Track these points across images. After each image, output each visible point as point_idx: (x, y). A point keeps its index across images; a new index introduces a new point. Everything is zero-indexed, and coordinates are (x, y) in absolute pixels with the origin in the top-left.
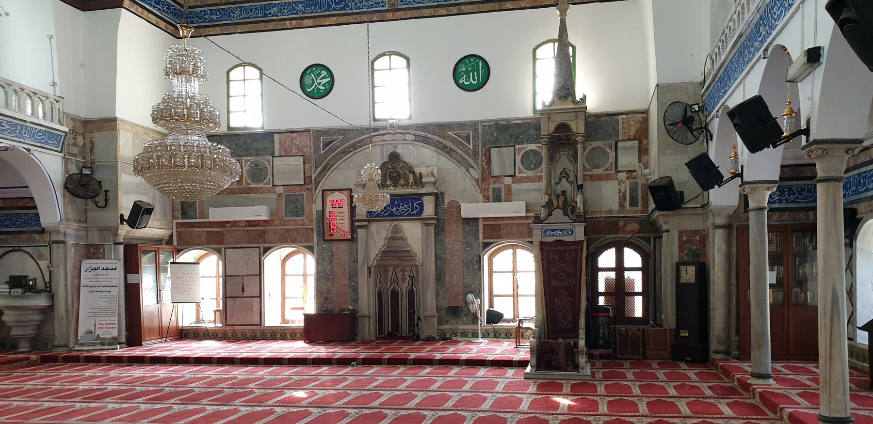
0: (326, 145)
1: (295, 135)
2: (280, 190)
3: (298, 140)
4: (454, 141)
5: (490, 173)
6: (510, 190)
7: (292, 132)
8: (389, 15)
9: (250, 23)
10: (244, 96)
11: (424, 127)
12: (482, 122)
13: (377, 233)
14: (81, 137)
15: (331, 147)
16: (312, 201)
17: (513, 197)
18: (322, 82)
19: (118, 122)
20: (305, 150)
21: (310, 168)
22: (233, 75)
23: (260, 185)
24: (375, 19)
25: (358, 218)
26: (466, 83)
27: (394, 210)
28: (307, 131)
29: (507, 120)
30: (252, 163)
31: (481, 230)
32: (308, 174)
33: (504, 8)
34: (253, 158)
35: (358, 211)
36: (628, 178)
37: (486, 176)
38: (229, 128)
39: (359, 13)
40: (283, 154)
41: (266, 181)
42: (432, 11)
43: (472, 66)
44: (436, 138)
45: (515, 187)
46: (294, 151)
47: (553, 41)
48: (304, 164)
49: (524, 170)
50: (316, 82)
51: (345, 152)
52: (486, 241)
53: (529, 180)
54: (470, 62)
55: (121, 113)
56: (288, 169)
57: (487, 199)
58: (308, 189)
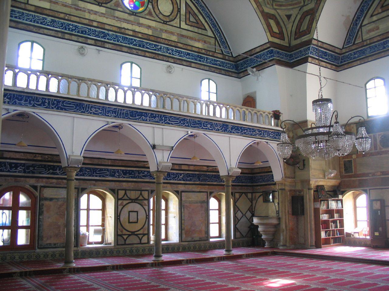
10: (376, 96)
14: (291, 132)
22: (368, 86)
30: (382, 136)
38: (368, 117)
55: (308, 118)
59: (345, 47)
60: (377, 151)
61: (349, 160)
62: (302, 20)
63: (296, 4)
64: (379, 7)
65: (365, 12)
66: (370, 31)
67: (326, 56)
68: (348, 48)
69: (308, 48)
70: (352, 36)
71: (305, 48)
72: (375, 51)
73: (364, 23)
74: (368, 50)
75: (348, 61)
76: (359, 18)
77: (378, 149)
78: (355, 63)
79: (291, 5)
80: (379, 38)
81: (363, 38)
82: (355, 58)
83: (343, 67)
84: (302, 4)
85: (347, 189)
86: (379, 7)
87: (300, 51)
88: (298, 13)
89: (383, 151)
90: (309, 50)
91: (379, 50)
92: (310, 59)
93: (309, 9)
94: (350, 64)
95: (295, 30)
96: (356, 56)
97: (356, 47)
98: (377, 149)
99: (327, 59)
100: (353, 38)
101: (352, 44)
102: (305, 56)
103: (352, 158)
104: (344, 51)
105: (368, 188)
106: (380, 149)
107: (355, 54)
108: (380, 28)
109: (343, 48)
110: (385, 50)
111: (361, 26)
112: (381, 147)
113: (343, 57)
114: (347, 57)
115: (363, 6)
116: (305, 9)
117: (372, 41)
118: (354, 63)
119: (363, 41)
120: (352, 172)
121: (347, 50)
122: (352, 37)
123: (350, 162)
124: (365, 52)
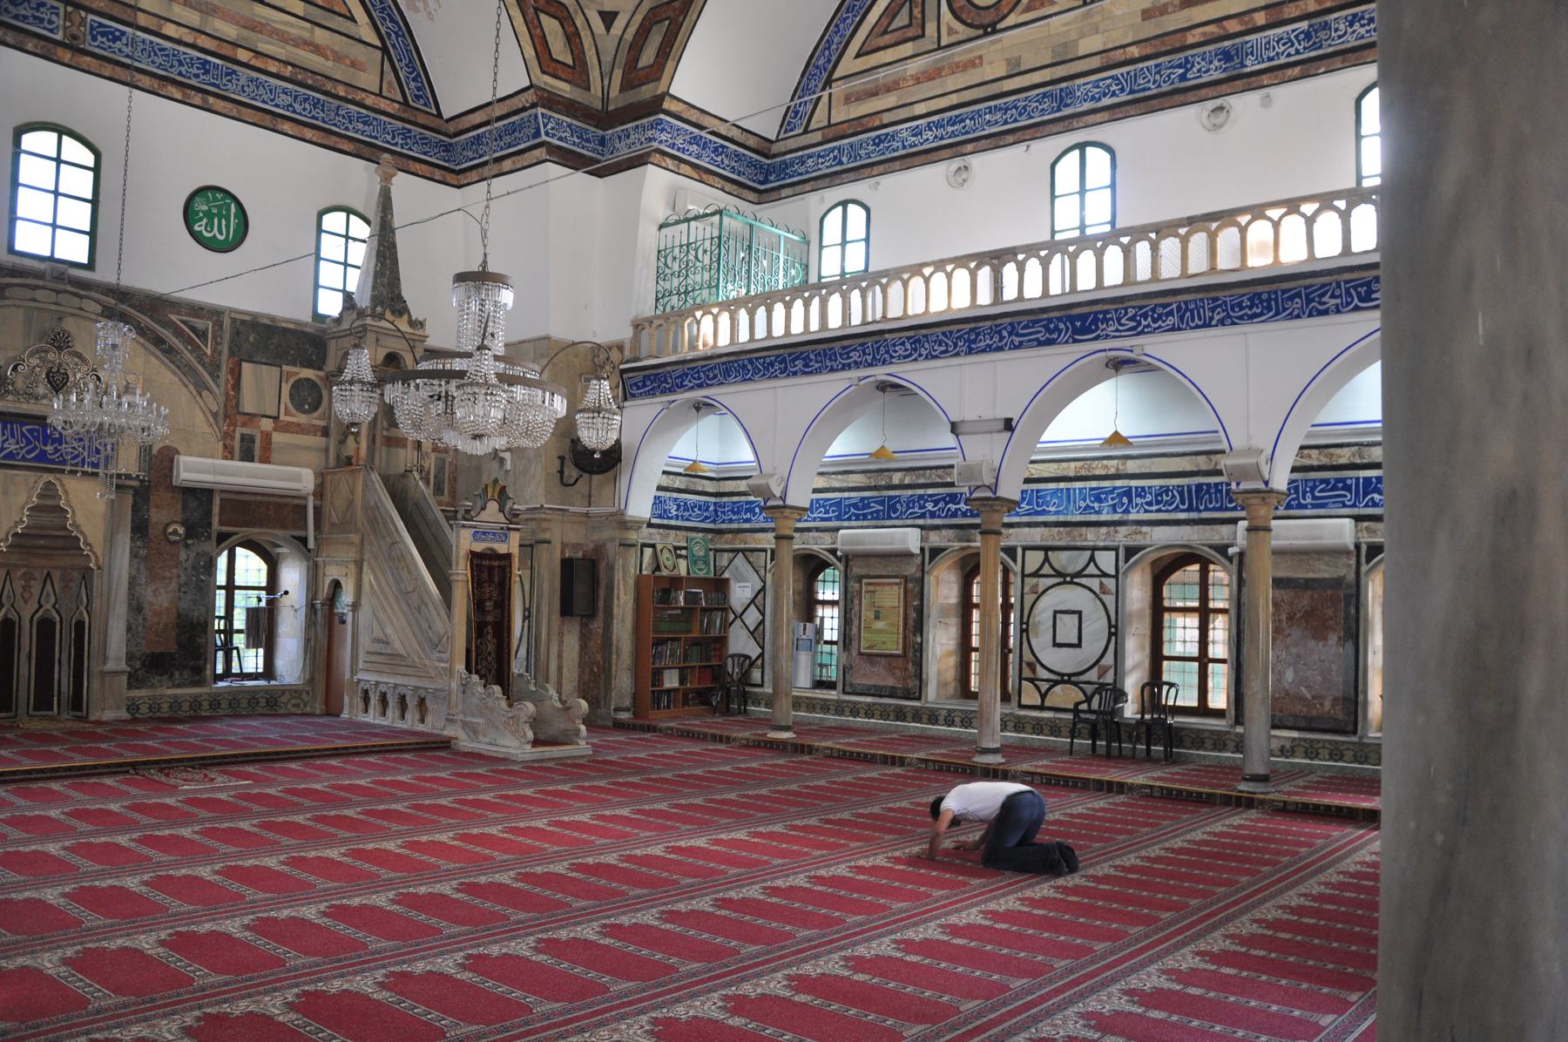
4: (178, 332)
5: (237, 404)
6: (270, 443)
11: (122, 294)
12: (232, 310)
17: (274, 456)
27: (49, 448)
29: (273, 319)
31: (216, 510)
33: (279, 127)
37: (231, 412)
44: (145, 320)
45: (278, 438)
47: (349, 211)
49: (293, 410)
54: (215, 199)
57: (229, 453)
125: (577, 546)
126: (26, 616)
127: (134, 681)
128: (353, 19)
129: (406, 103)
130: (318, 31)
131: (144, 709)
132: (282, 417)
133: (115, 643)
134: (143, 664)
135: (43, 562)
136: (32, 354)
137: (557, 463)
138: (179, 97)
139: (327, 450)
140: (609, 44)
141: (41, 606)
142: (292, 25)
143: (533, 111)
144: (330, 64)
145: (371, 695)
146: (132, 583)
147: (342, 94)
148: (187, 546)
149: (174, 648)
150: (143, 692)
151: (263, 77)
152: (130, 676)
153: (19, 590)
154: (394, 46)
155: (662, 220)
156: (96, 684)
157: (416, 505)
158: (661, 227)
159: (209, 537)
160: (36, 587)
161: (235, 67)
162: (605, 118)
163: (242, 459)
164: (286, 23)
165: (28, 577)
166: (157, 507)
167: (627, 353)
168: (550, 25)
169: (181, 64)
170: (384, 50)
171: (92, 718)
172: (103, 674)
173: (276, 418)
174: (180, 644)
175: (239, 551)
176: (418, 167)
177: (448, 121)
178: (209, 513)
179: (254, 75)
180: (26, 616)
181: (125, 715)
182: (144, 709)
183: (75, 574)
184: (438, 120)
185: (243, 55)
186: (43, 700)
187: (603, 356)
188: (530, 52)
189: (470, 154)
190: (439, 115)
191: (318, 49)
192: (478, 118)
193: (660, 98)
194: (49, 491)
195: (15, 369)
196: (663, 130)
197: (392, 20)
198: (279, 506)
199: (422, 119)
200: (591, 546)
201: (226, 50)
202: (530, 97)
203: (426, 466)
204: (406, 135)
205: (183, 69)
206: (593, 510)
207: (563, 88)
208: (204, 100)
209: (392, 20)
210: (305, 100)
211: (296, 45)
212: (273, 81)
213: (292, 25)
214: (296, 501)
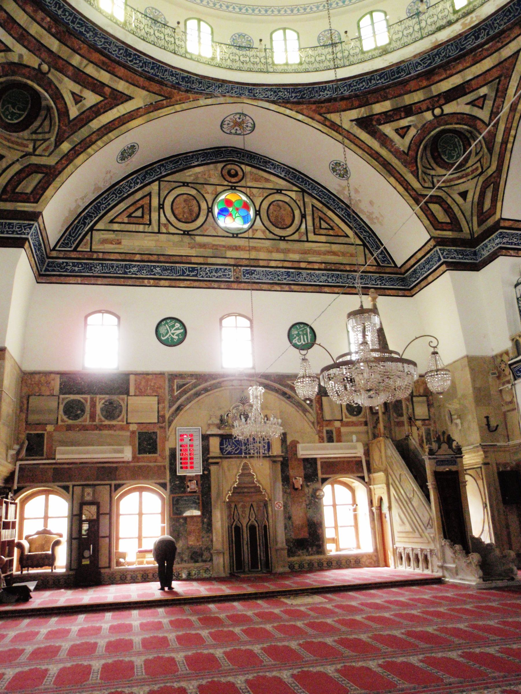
0: (180, 387)
1: (150, 377)
2: (133, 427)
3: (154, 381)
5: (323, 417)
7: (148, 374)
8: (235, 285)
9: (110, 277)
11: (266, 376)
13: (229, 470)
15: (184, 389)
16: (165, 439)
17: (343, 438)
18: (176, 332)
19: (6, 351)
20: (160, 391)
21: (164, 408)
23: (114, 423)
24: (222, 286)
25: (211, 455)
26: (299, 344)
28: (162, 374)
30: (106, 402)
32: (161, 413)
33: (323, 291)
34: (107, 397)
35: (212, 449)
36: (423, 425)
39: (209, 281)
40: (138, 393)
41: (120, 419)
42: (269, 287)
43: (302, 331)
44: (278, 386)
45: (343, 430)
46: (149, 391)
48: (158, 404)
50: (171, 332)
51: (197, 394)
52: (325, 476)
53: (353, 424)
54: (300, 328)
56: (142, 409)
57: (321, 440)
58: (161, 427)
59: (57, 248)
60: (94, 423)
61: (37, 434)
62: (24, 175)
63: (17, 144)
64: (126, 214)
65: (102, 212)
66: (104, 241)
67: (39, 250)
68: (63, 253)
69: (29, 225)
70: (74, 237)
71: (21, 222)
72: (110, 273)
73: (97, 227)
74: (98, 267)
75: (59, 271)
76: (89, 216)
77: (97, 420)
78: (72, 280)
79: (8, 140)
80: (118, 257)
81: (93, 247)
82: (74, 271)
83: (48, 278)
84: (30, 149)
85: (28, 484)
86: (126, 214)
87: (10, 224)
88: (18, 160)
89: (105, 425)
90: (30, 228)
91: (117, 273)
92: (27, 244)
93: (42, 163)
94: (62, 278)
95: (4, 184)
96: (77, 269)
97: (78, 256)
98: (95, 421)
99: (37, 255)
100: (75, 240)
101: (72, 249)
102: (18, 236)
103: (46, 430)
104: (54, 254)
105: (70, 484)
106: (100, 419)
107: (74, 266)
108: (123, 243)
109: (54, 249)
110: (126, 276)
111: (92, 229)
112: (103, 419)
113: (53, 263)
114: (59, 265)
115: (99, 202)
116: (34, 160)
117: (107, 256)
118: (71, 278)
119: (91, 251)
120: (42, 455)
121: (61, 256)
122: (73, 239)
123: (41, 436)
124: (93, 268)
125: (505, 465)
126: (244, 525)
127: (291, 553)
128: (347, 236)
129: (379, 265)
130: (334, 246)
131: (297, 566)
132: (344, 419)
133: (280, 535)
134: (294, 545)
135: (248, 499)
136: (233, 408)
137: (485, 420)
138: (279, 289)
139: (367, 432)
140: (467, 206)
141: (250, 520)
142: (322, 247)
143: (435, 249)
144: (341, 258)
145: (403, 555)
146: (285, 506)
147: (348, 269)
148: (308, 486)
149: (307, 536)
150: (295, 559)
151: (313, 272)
152: (289, 551)
153: (240, 513)
154: (368, 242)
155: (515, 283)
156: (273, 553)
157: (413, 453)
158: (516, 286)
159: (318, 480)
160: (247, 510)
161: (300, 271)
162: (474, 242)
163: (328, 442)
164: (319, 247)
165: (244, 507)
166: (293, 469)
167: (511, 355)
168: (435, 208)
169: (278, 276)
170: (364, 245)
171: (274, 572)
172: (277, 550)
173: (341, 420)
174: (310, 534)
175: (337, 487)
176: (390, 292)
177: (400, 268)
178: (316, 469)
179: (309, 272)
180: (244, 525)
181: (287, 569)
182: (297, 566)
183: (262, 504)
184: (395, 269)
185: (303, 265)
186: (254, 564)
187: (499, 360)
188: (427, 222)
189: (413, 279)
190: (396, 266)
191: (334, 253)
192: (412, 261)
193: (498, 222)
194: (245, 467)
195: (227, 415)
196: (503, 237)
197: (366, 231)
198: (348, 462)
199: (388, 270)
200: (514, 463)
201: (296, 265)
202: (432, 243)
203: (421, 433)
204: (381, 279)
205: (279, 278)
206: (511, 443)
207: (448, 234)
208: (290, 288)
209: (366, 231)
210: (333, 276)
211: (325, 254)
212: (317, 272)
213: (322, 247)
214: (357, 459)
